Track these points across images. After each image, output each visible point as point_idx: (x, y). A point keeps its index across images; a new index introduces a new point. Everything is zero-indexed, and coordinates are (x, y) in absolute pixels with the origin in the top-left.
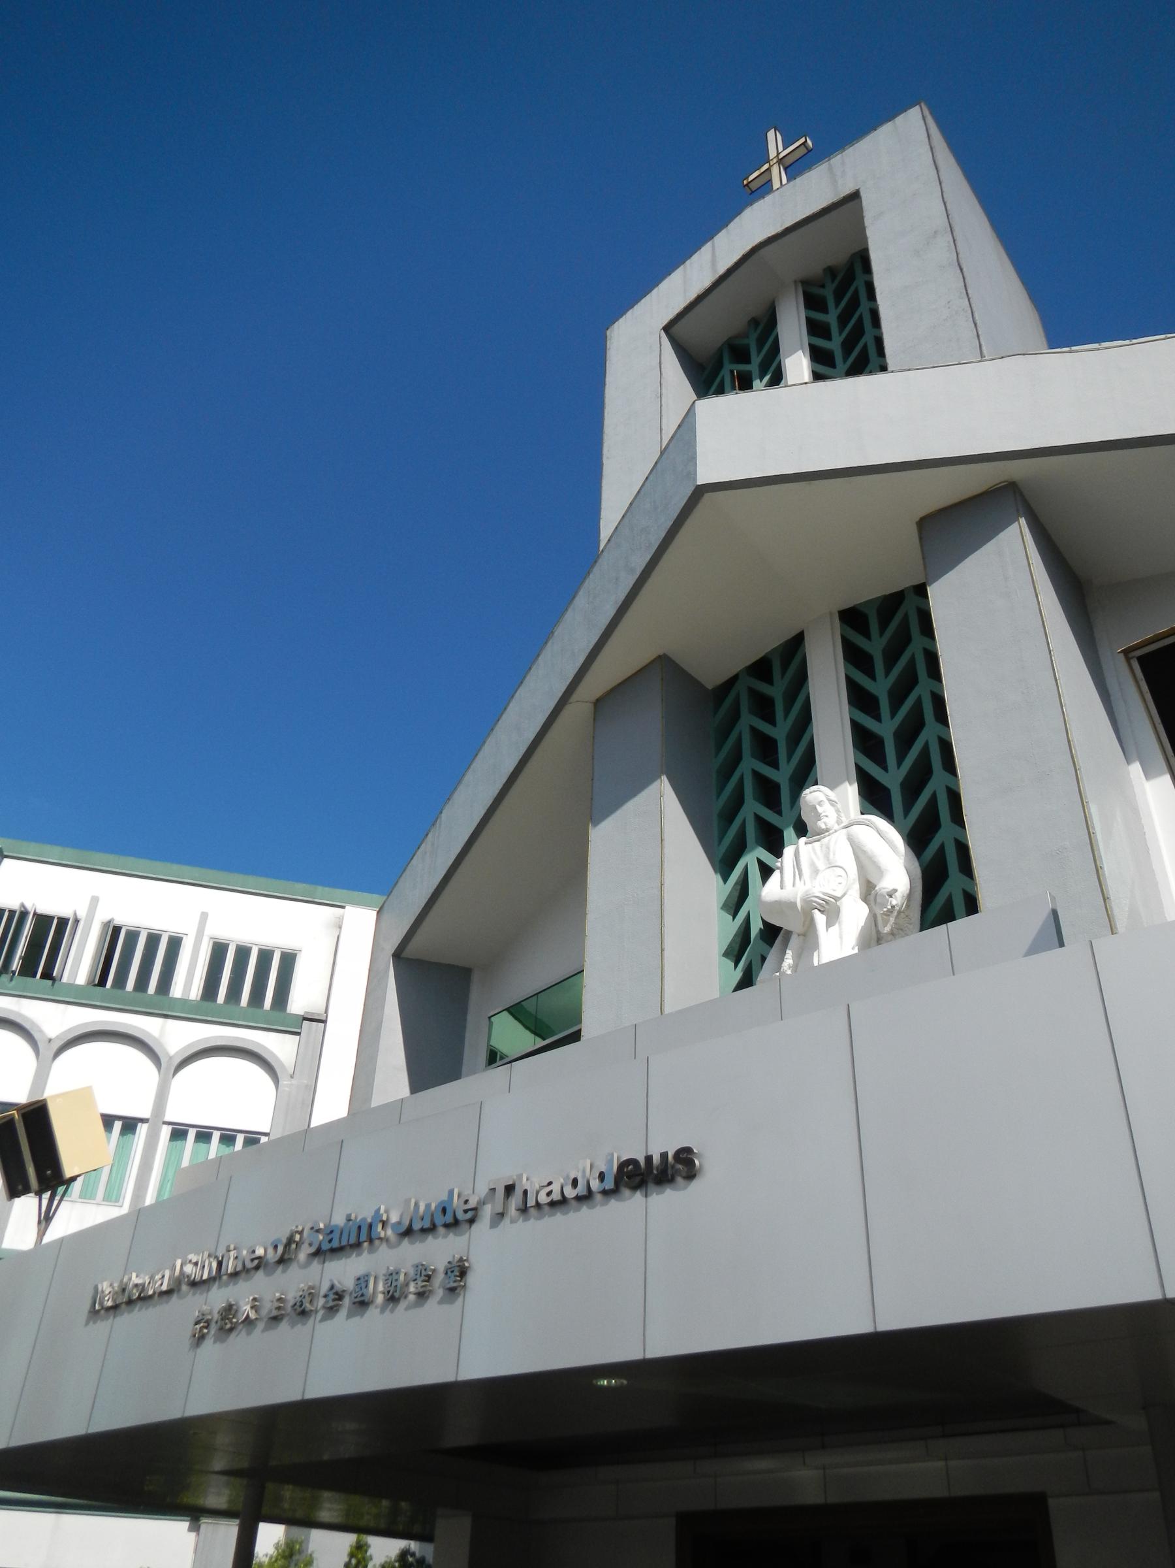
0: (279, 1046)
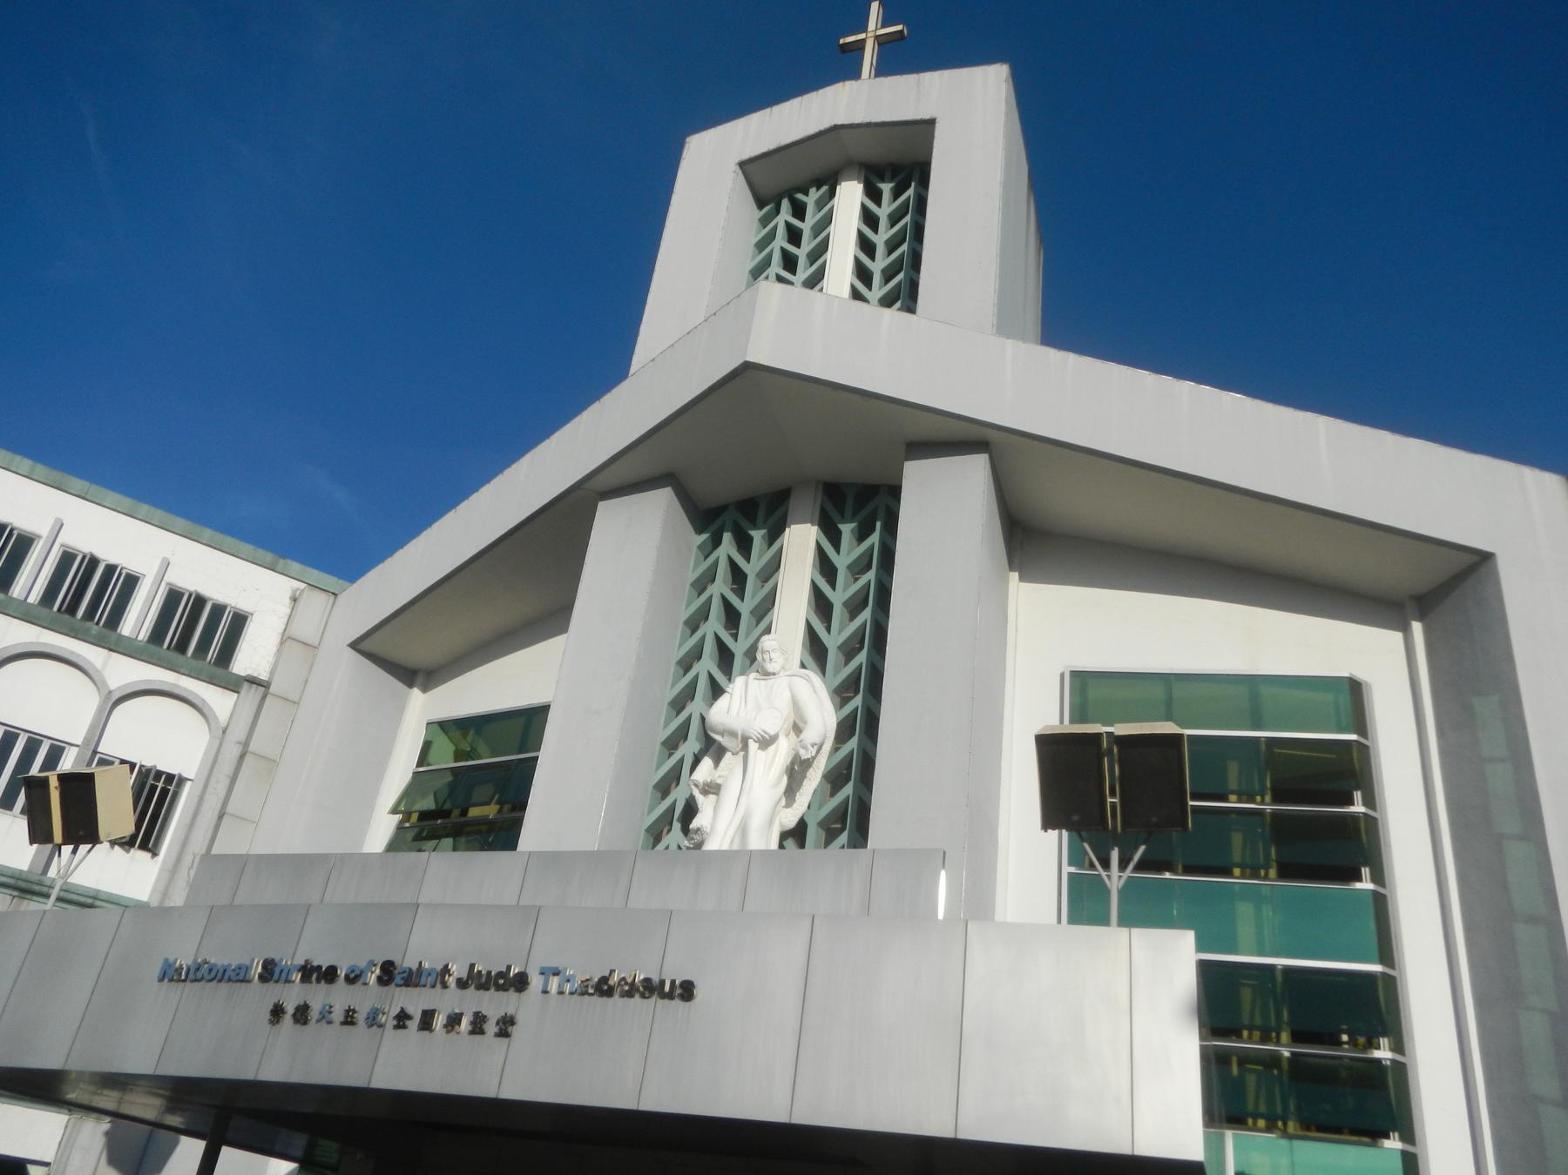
0: (220, 701)
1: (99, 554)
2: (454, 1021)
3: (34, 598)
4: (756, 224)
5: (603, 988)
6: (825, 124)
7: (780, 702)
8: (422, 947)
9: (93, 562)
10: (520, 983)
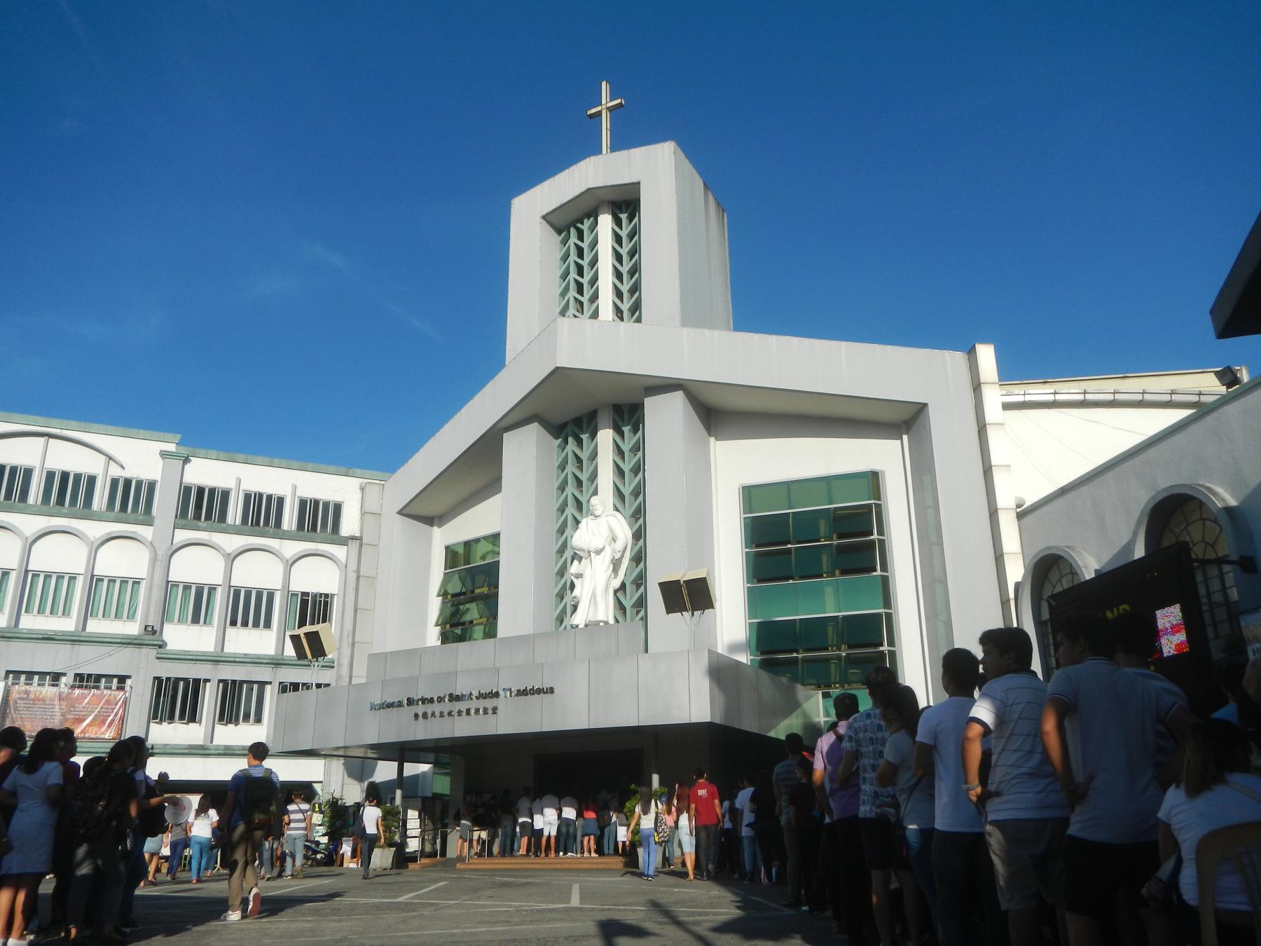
0: (339, 552)
1: (262, 491)
2: (477, 711)
3: (238, 522)
4: (559, 245)
5: (523, 693)
6: (584, 189)
7: (603, 530)
8: (461, 688)
9: (261, 495)
10: (497, 695)
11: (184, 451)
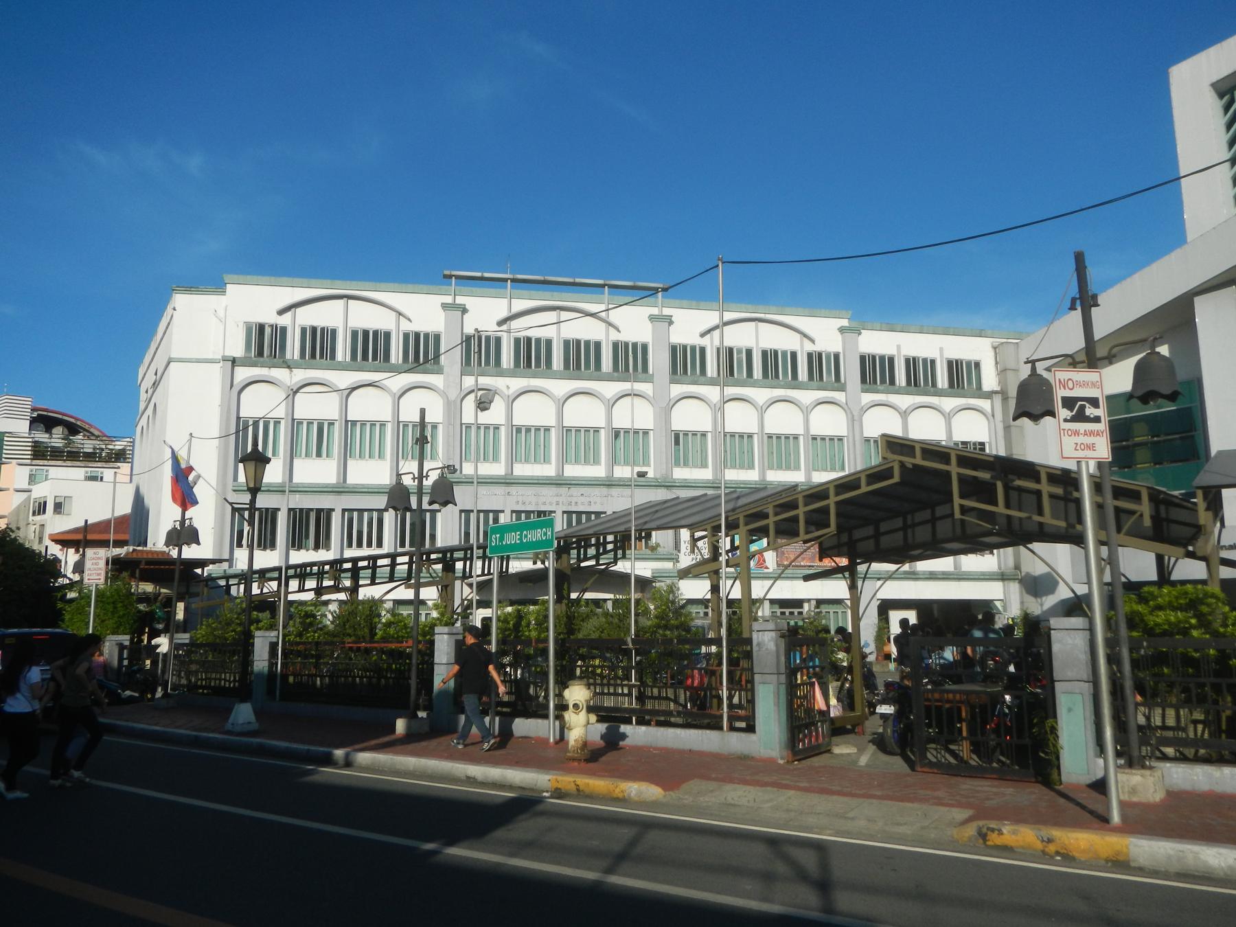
0: (985, 404)
11: (854, 324)
